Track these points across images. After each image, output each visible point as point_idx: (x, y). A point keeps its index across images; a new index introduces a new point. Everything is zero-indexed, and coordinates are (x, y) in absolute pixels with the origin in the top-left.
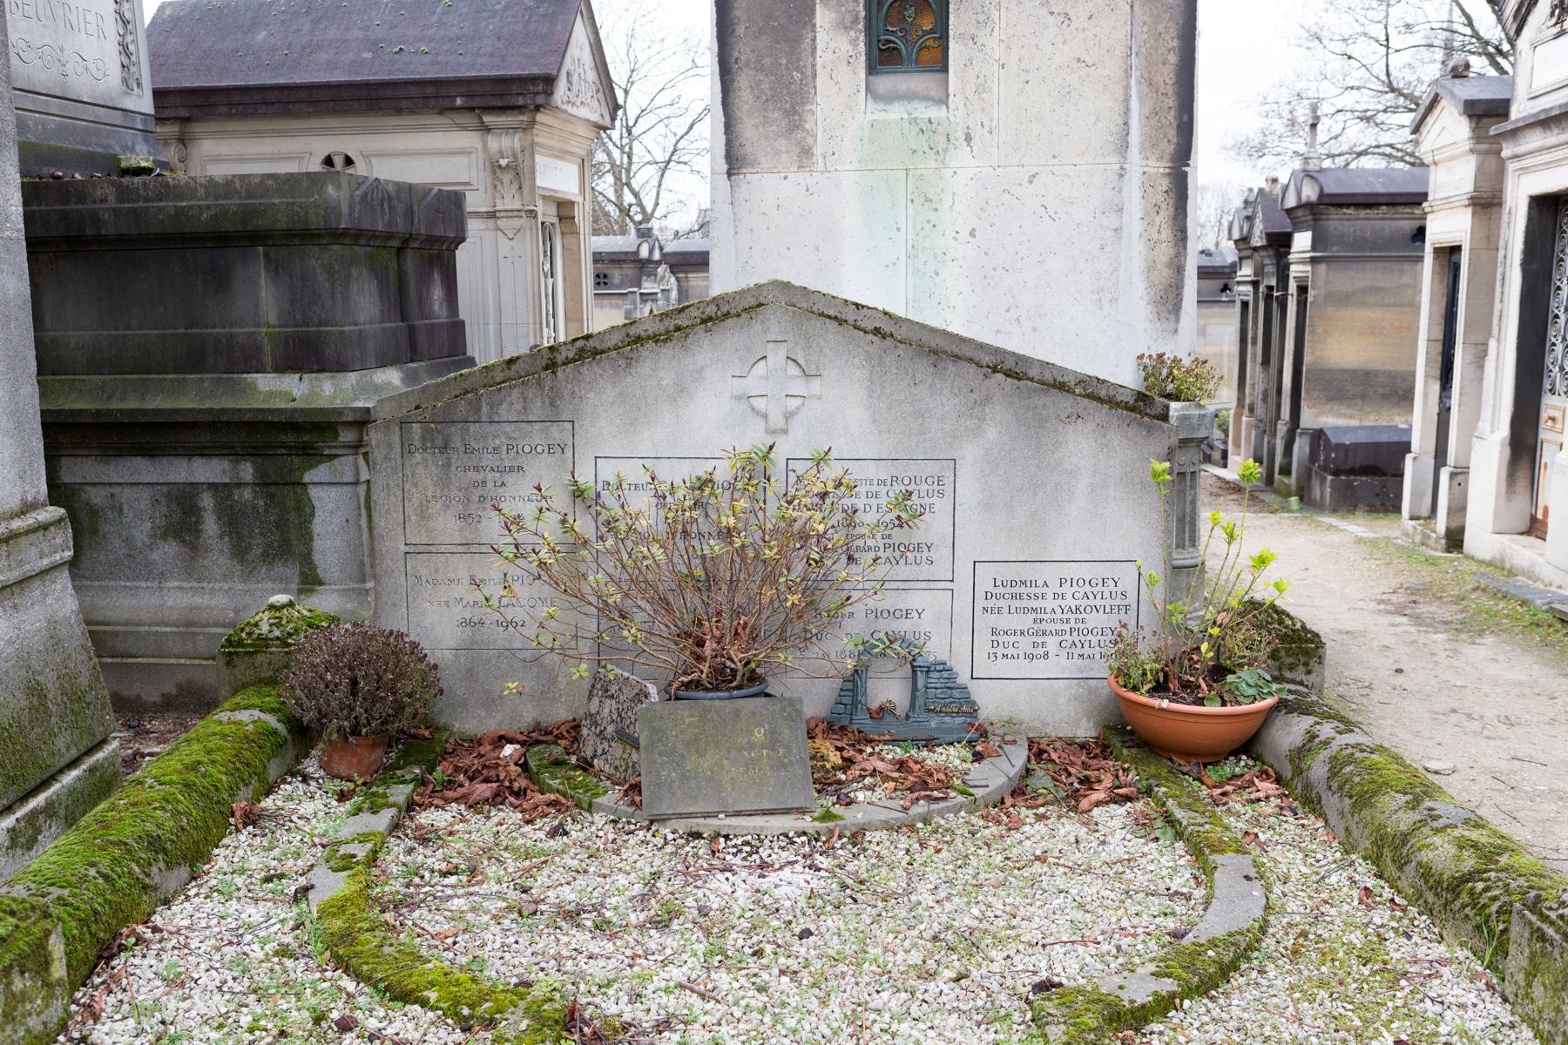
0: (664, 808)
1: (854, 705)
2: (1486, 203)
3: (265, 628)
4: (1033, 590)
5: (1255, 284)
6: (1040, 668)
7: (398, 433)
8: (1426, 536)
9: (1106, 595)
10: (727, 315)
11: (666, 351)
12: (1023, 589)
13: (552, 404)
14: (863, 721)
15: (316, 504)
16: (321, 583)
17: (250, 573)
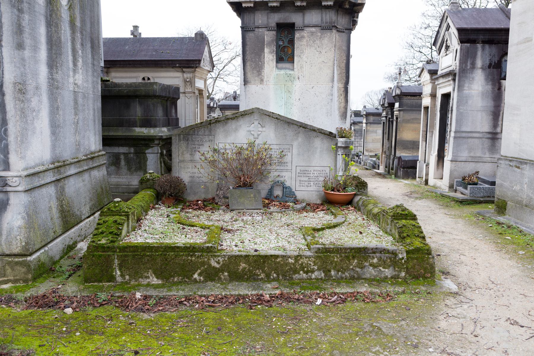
0: (234, 208)
1: (271, 195)
2: (433, 96)
3: (149, 177)
5: (386, 117)
6: (309, 189)
8: (421, 182)
10: (246, 114)
11: (234, 121)
14: (272, 198)
17: (132, 174)
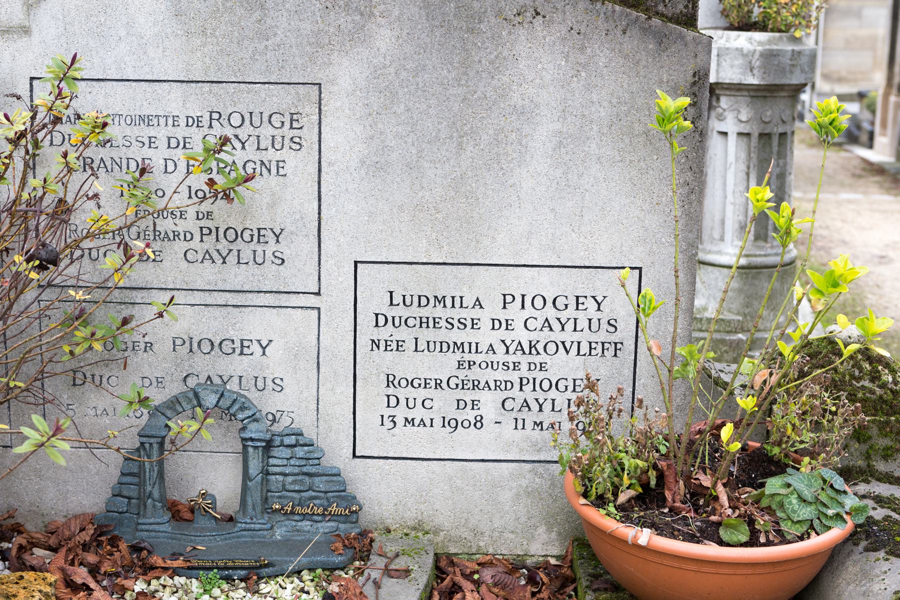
1: (143, 498)
4: (457, 314)
9: (583, 324)
12: (439, 312)
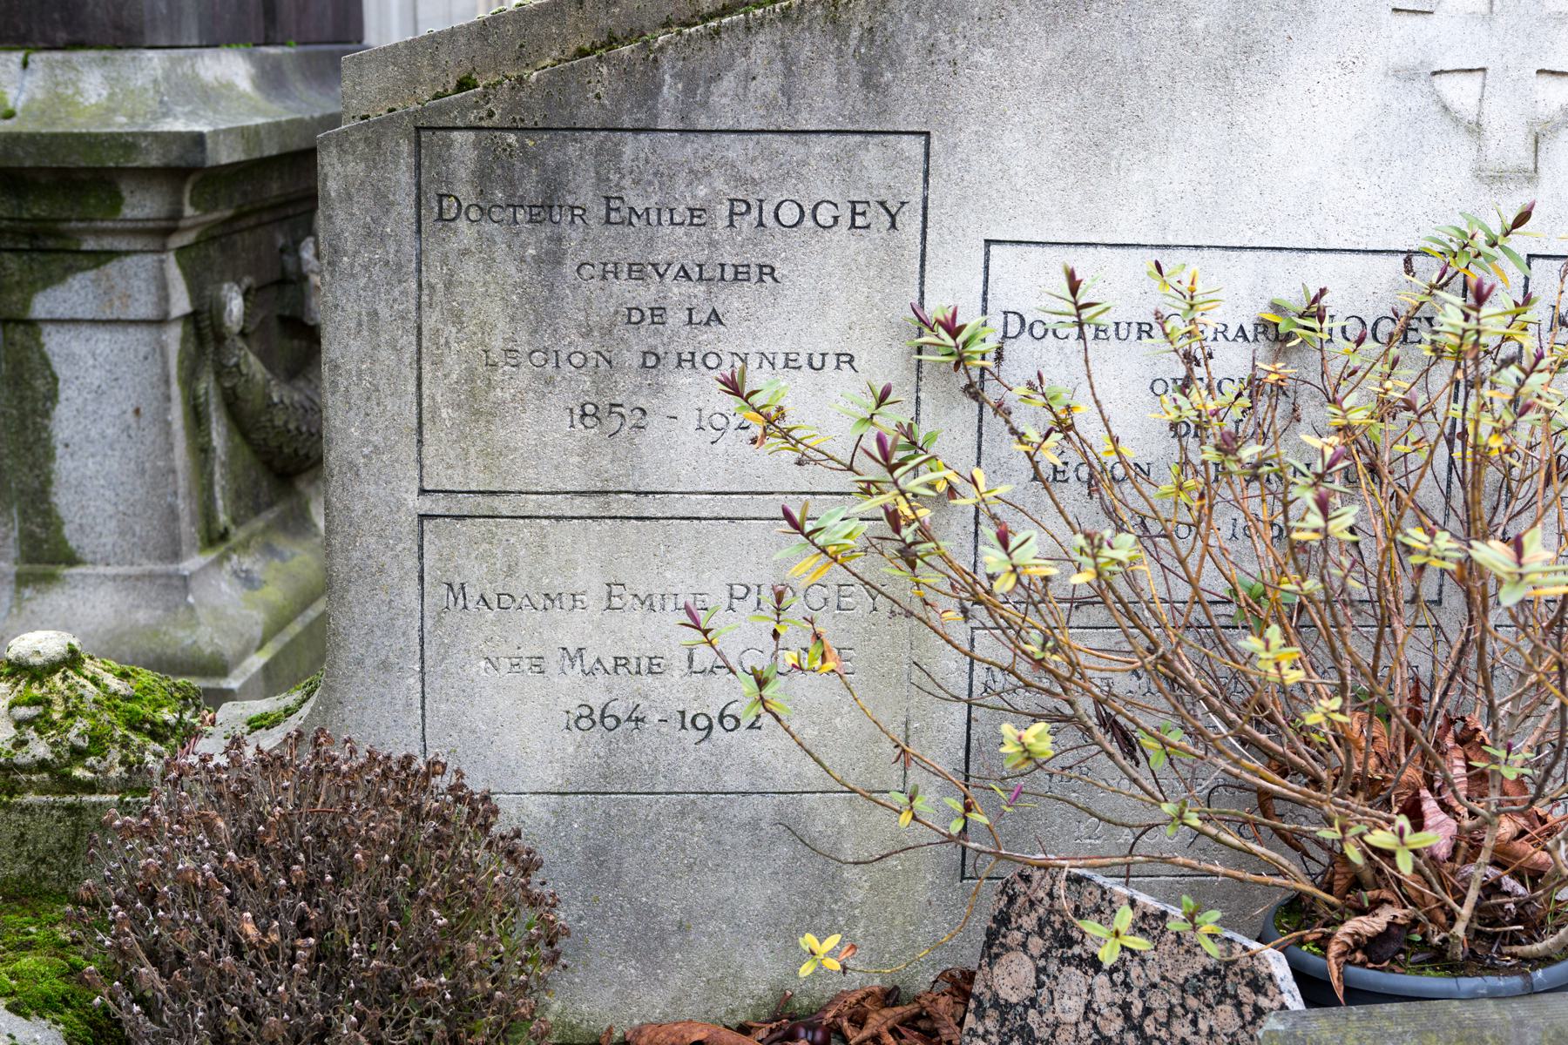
7: (406, 160)
13: (868, 82)
15: (62, 370)
16: (72, 560)
